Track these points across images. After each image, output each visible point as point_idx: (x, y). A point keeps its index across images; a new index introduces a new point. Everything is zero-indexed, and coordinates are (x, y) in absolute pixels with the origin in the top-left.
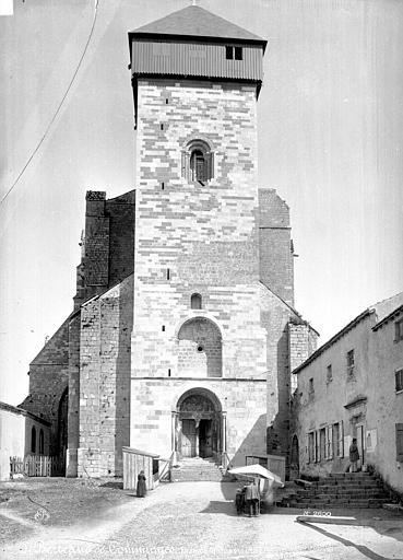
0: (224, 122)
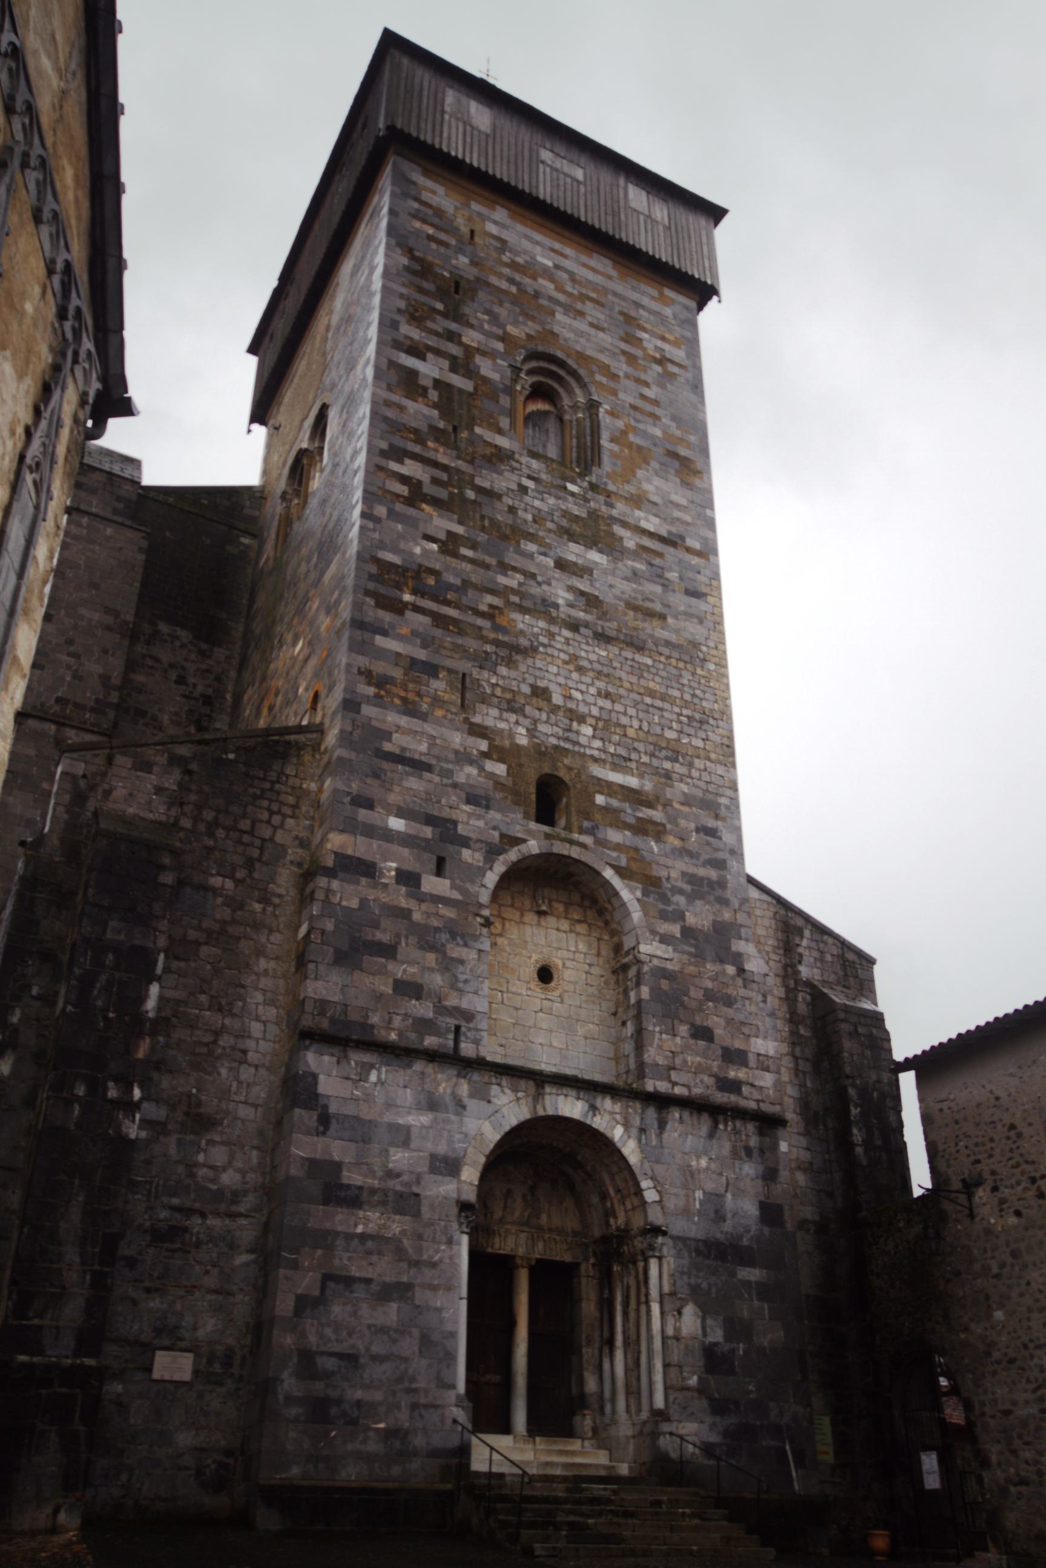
0: (623, 346)
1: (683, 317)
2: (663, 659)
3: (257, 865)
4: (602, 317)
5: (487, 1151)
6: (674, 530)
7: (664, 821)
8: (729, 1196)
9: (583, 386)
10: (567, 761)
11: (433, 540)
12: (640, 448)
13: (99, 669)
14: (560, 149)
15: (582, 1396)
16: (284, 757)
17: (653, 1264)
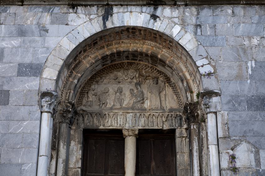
5: (65, 57)
17: (211, 120)
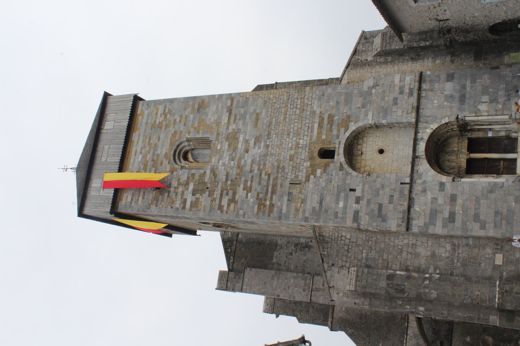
0: (163, 129)
1: (147, 107)
2: (272, 114)
3: (358, 243)
4: (155, 137)
6: (225, 110)
7: (328, 114)
8: (445, 93)
9: (181, 143)
10: (313, 149)
11: (247, 195)
12: (199, 123)
13: (292, 280)
14: (98, 154)
15: (506, 136)
16: (323, 236)
17: (467, 119)
